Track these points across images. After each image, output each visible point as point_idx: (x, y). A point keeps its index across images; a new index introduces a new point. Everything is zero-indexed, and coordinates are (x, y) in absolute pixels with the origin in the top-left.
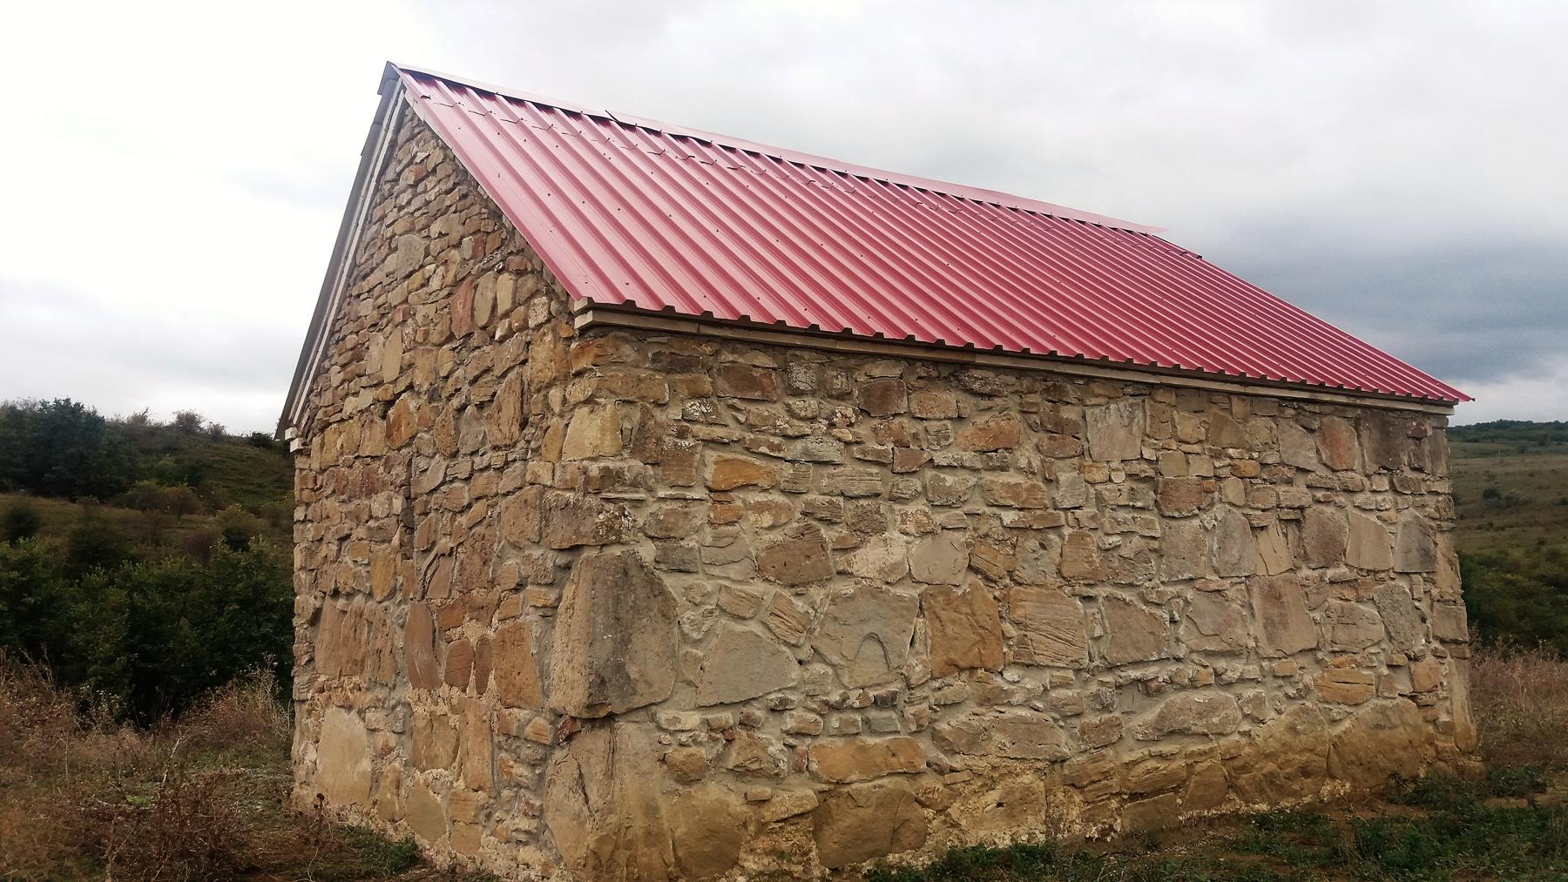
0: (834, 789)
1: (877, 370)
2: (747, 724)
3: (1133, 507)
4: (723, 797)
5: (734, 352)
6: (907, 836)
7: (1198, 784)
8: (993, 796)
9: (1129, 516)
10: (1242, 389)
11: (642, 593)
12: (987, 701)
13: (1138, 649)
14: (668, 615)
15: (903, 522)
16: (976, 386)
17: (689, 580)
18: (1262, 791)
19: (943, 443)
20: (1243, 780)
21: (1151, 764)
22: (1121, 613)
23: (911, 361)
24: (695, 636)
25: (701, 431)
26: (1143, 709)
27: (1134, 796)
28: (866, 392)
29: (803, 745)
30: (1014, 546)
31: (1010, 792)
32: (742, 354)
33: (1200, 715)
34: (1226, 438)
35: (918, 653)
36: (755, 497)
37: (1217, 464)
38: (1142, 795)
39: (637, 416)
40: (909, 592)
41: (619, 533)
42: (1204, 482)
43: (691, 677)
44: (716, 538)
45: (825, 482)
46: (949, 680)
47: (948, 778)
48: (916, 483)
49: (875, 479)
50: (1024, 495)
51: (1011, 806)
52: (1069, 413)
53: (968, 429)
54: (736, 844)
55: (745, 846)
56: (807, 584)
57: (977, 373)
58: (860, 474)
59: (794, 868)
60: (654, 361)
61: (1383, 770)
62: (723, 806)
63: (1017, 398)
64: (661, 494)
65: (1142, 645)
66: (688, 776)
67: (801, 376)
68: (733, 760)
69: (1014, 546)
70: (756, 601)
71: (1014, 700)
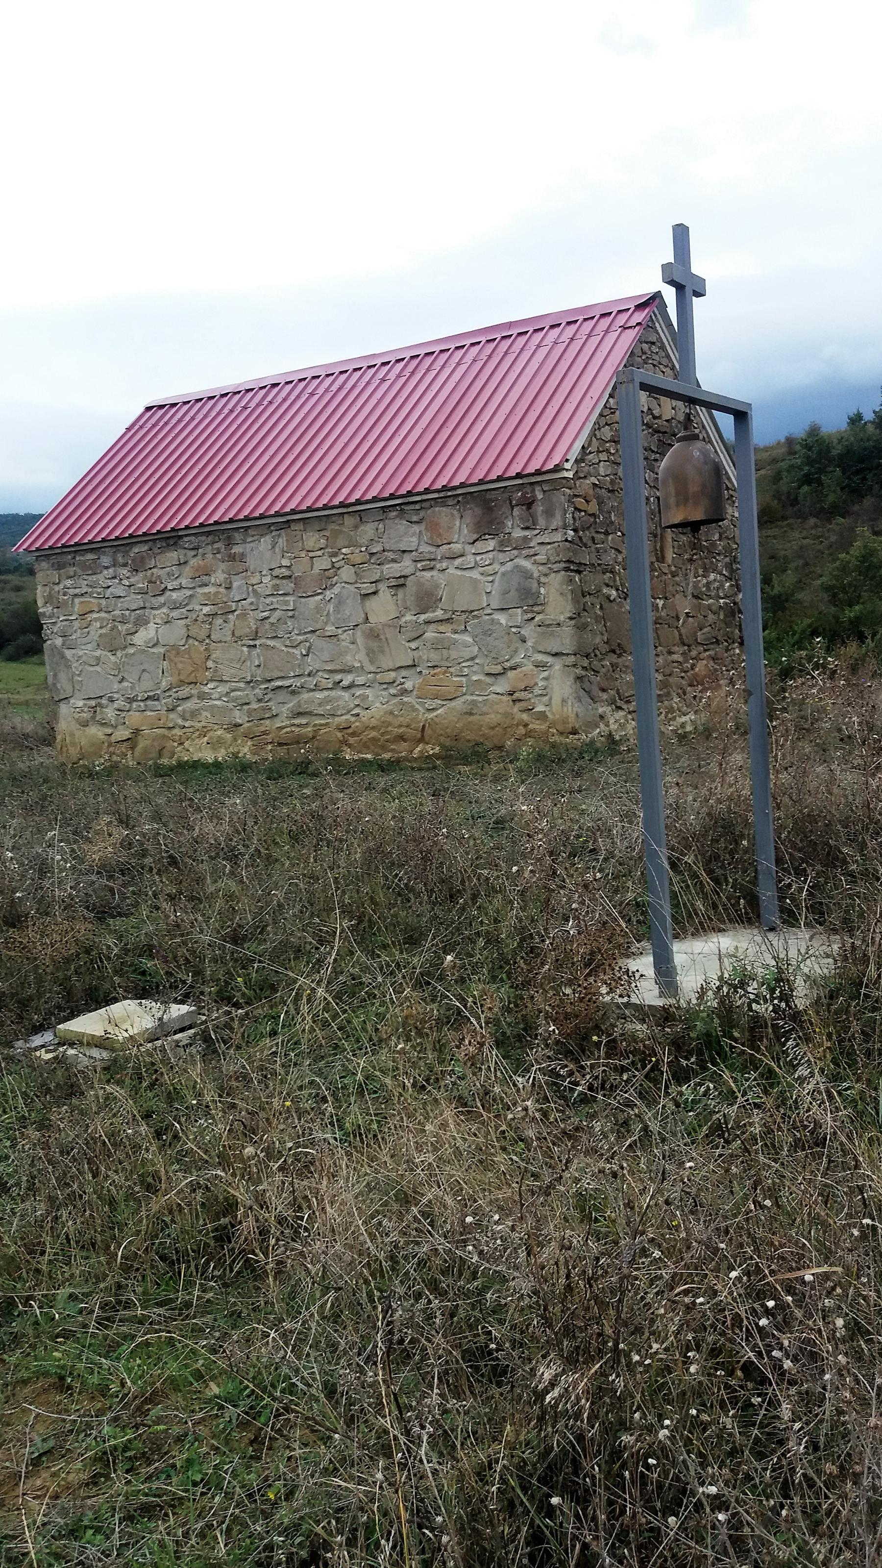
0: (137, 732)
2: (100, 705)
5: (81, 555)
6: (166, 753)
12: (202, 696)
14: (69, 667)
16: (186, 546)
18: (368, 748)
20: (352, 740)
24: (77, 673)
25: (72, 591)
26: (291, 701)
27: (280, 744)
30: (210, 624)
31: (211, 738)
32: (83, 555)
33: (320, 705)
34: (340, 543)
36: (95, 615)
37: (334, 560)
38: (286, 744)
40: (161, 650)
46: (182, 688)
47: (184, 730)
48: (162, 599)
50: (212, 598)
52: (236, 549)
56: (116, 650)
57: (186, 539)
61: (469, 741)
63: (210, 547)
67: (105, 560)
68: (97, 719)
69: (210, 624)
70: (98, 659)
71: (213, 697)
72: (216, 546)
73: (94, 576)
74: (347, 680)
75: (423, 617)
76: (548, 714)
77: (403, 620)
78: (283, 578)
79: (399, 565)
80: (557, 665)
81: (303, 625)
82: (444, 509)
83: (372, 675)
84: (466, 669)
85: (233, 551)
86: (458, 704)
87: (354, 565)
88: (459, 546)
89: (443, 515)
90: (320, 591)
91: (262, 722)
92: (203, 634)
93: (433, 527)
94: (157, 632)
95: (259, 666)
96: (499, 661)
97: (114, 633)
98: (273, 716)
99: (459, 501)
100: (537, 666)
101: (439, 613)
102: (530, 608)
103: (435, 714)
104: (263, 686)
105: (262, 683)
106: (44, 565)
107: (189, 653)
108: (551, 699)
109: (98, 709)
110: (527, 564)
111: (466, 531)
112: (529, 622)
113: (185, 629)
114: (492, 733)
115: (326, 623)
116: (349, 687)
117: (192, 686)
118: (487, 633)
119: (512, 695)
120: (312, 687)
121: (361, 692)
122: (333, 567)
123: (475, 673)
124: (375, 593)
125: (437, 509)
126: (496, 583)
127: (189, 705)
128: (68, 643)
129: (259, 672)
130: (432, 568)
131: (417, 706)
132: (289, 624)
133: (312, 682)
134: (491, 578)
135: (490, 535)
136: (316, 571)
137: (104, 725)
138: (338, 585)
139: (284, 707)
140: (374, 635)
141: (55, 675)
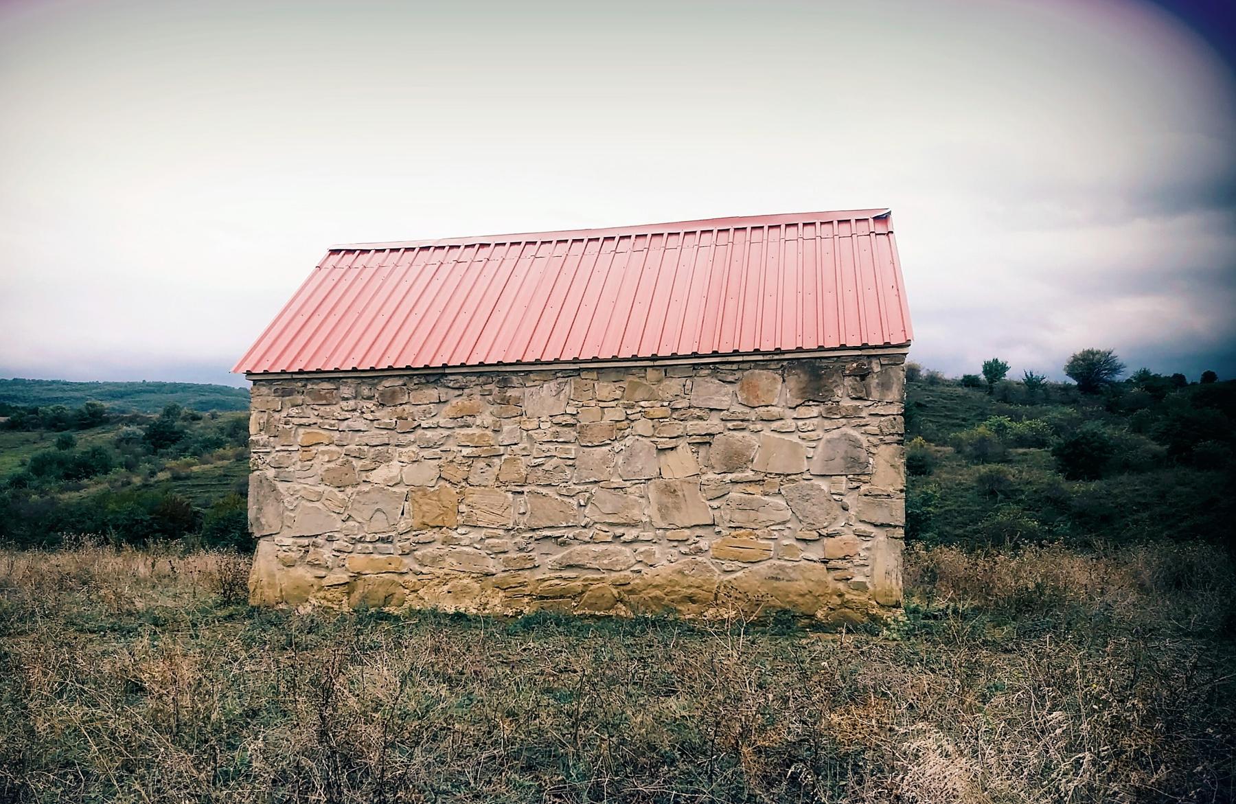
1: (387, 383)
2: (315, 545)
3: (556, 442)
4: (304, 574)
5: (312, 384)
7: (590, 597)
8: (446, 588)
9: (553, 447)
10: (651, 363)
11: (267, 490)
13: (551, 520)
14: (279, 500)
15: (400, 456)
16: (451, 385)
17: (289, 484)
19: (428, 416)
21: (557, 582)
22: (540, 500)
23: (411, 376)
25: (296, 421)
27: (542, 598)
28: (381, 394)
29: (342, 556)
32: (317, 384)
34: (638, 396)
35: (405, 518)
38: (547, 598)
39: (265, 416)
41: (258, 466)
42: (618, 424)
43: (289, 525)
44: (302, 467)
45: (357, 439)
46: (424, 532)
47: (420, 577)
48: (411, 437)
49: (384, 436)
50: (476, 440)
51: (456, 593)
53: (447, 407)
54: (308, 593)
55: (312, 595)
58: (377, 435)
59: (334, 606)
60: (274, 393)
62: (302, 577)
63: (479, 388)
64: (277, 449)
65: (552, 518)
66: (290, 565)
67: (346, 391)
70: (320, 494)
71: (462, 543)
72: (487, 387)
73: (327, 407)
74: (630, 534)
75: (730, 477)
76: (868, 585)
77: (704, 478)
78: (566, 425)
79: (706, 422)
80: (881, 536)
81: (584, 475)
82: (765, 372)
83: (661, 531)
84: (775, 533)
85: (508, 394)
86: (762, 568)
87: (652, 419)
88: (779, 409)
89: (764, 378)
90: (609, 442)
91: (520, 572)
92: (459, 477)
93: (749, 388)
94: (401, 471)
95: (524, 513)
96: (814, 527)
97: (345, 469)
98: (535, 567)
99: (782, 366)
100: (859, 536)
101: (749, 474)
102: (856, 477)
103: (734, 576)
104: (528, 535)
105: (525, 531)
106: (264, 390)
107: (438, 496)
108: (872, 570)
109: (312, 549)
110: (855, 433)
111: (788, 395)
112: (854, 491)
113: (438, 470)
114: (801, 600)
115: (612, 475)
116: (631, 542)
117: (435, 530)
118: (805, 498)
119: (827, 562)
120: (587, 539)
121: (647, 548)
122: (627, 419)
123: (786, 537)
124: (672, 449)
125: (757, 371)
126: (820, 449)
127: (430, 550)
128: (282, 475)
129: (525, 518)
130: (744, 429)
131: (712, 567)
132: (568, 472)
133: (588, 534)
134: (814, 444)
135: (814, 401)
136: (606, 420)
137: (314, 565)
138: (630, 437)
139: (548, 559)
140: (669, 490)
141: (260, 509)
